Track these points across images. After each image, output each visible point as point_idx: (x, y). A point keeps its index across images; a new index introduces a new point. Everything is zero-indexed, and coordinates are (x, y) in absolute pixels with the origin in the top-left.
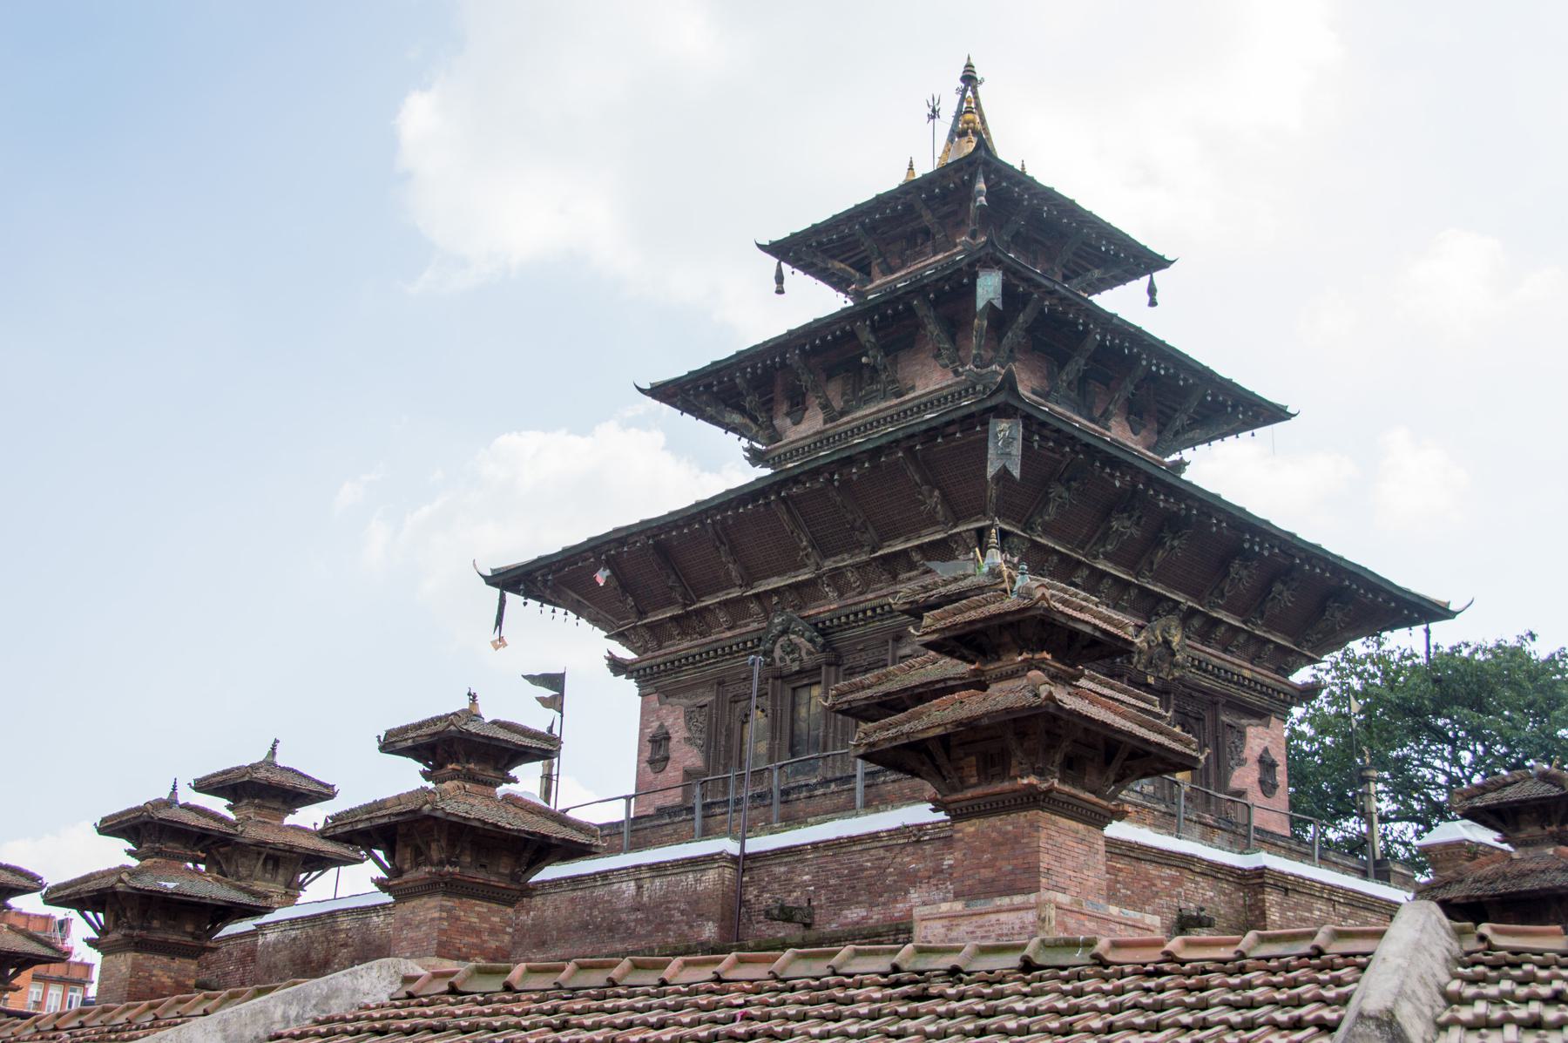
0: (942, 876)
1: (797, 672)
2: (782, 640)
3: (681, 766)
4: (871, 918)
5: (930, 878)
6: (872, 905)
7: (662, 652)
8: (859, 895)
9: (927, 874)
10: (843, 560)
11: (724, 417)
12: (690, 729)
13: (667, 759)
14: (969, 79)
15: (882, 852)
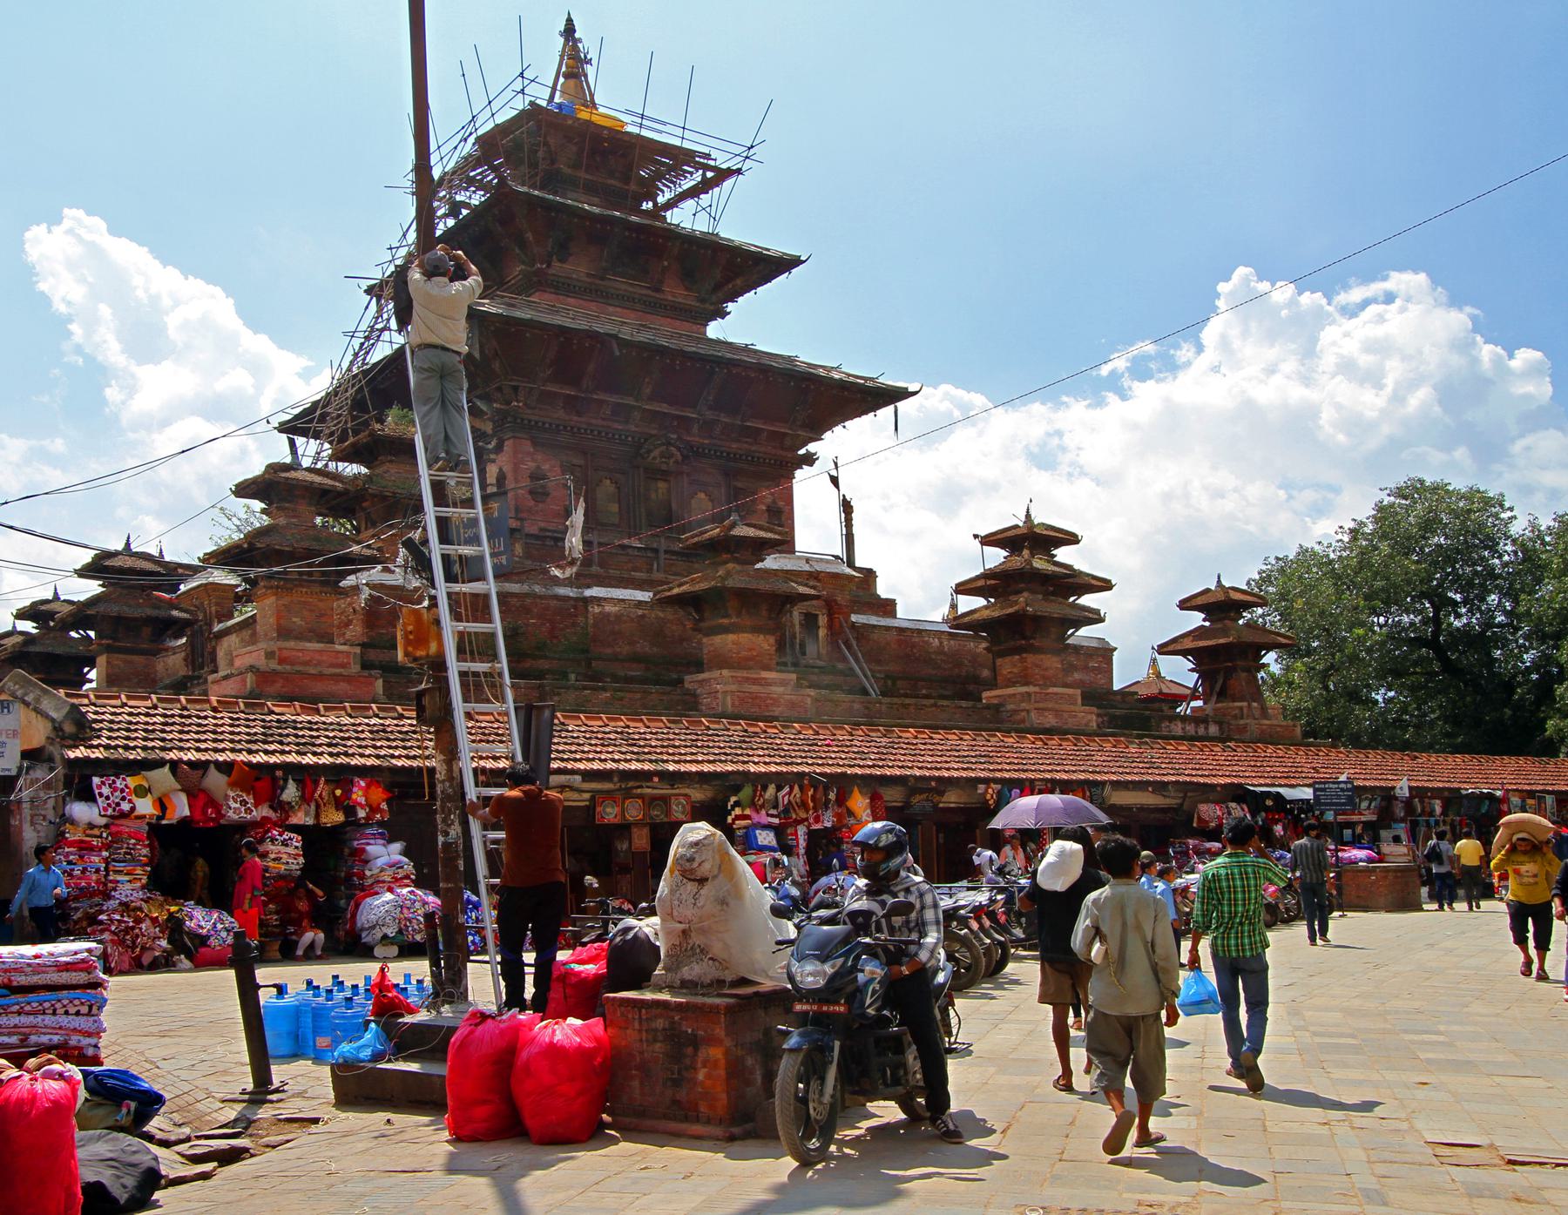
2: (663, 448)
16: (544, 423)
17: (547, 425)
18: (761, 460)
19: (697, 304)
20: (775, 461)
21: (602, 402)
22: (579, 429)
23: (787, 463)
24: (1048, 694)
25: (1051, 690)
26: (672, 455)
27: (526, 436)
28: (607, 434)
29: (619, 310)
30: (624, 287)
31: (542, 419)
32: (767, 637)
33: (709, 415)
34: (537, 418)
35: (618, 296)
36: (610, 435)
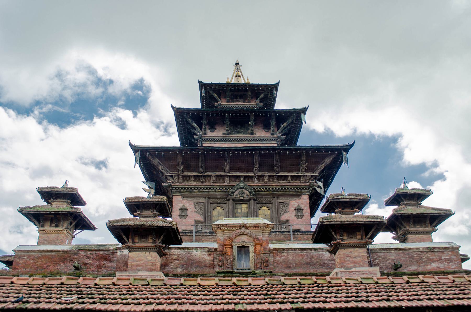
0: (442, 261)
1: (242, 200)
2: (239, 190)
3: (193, 219)
4: (419, 269)
5: (438, 261)
6: (419, 266)
7: (184, 184)
8: (413, 263)
9: (437, 260)
10: (265, 173)
11: (192, 123)
12: (196, 209)
13: (187, 216)
14: (237, 64)
15: (420, 253)
16: (185, 188)
17: (186, 189)
18: (289, 189)
19: (269, 136)
20: (297, 188)
21: (210, 176)
22: (201, 188)
23: (303, 188)
24: (352, 272)
25: (354, 269)
26: (244, 193)
27: (180, 194)
28: (213, 188)
29: (237, 144)
30: (236, 135)
31: (184, 186)
32: (151, 253)
33: (260, 173)
34: (181, 186)
35: (235, 139)
36: (215, 189)
